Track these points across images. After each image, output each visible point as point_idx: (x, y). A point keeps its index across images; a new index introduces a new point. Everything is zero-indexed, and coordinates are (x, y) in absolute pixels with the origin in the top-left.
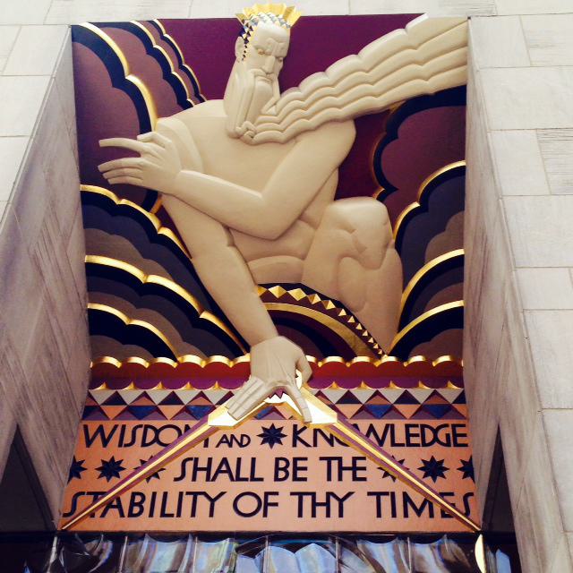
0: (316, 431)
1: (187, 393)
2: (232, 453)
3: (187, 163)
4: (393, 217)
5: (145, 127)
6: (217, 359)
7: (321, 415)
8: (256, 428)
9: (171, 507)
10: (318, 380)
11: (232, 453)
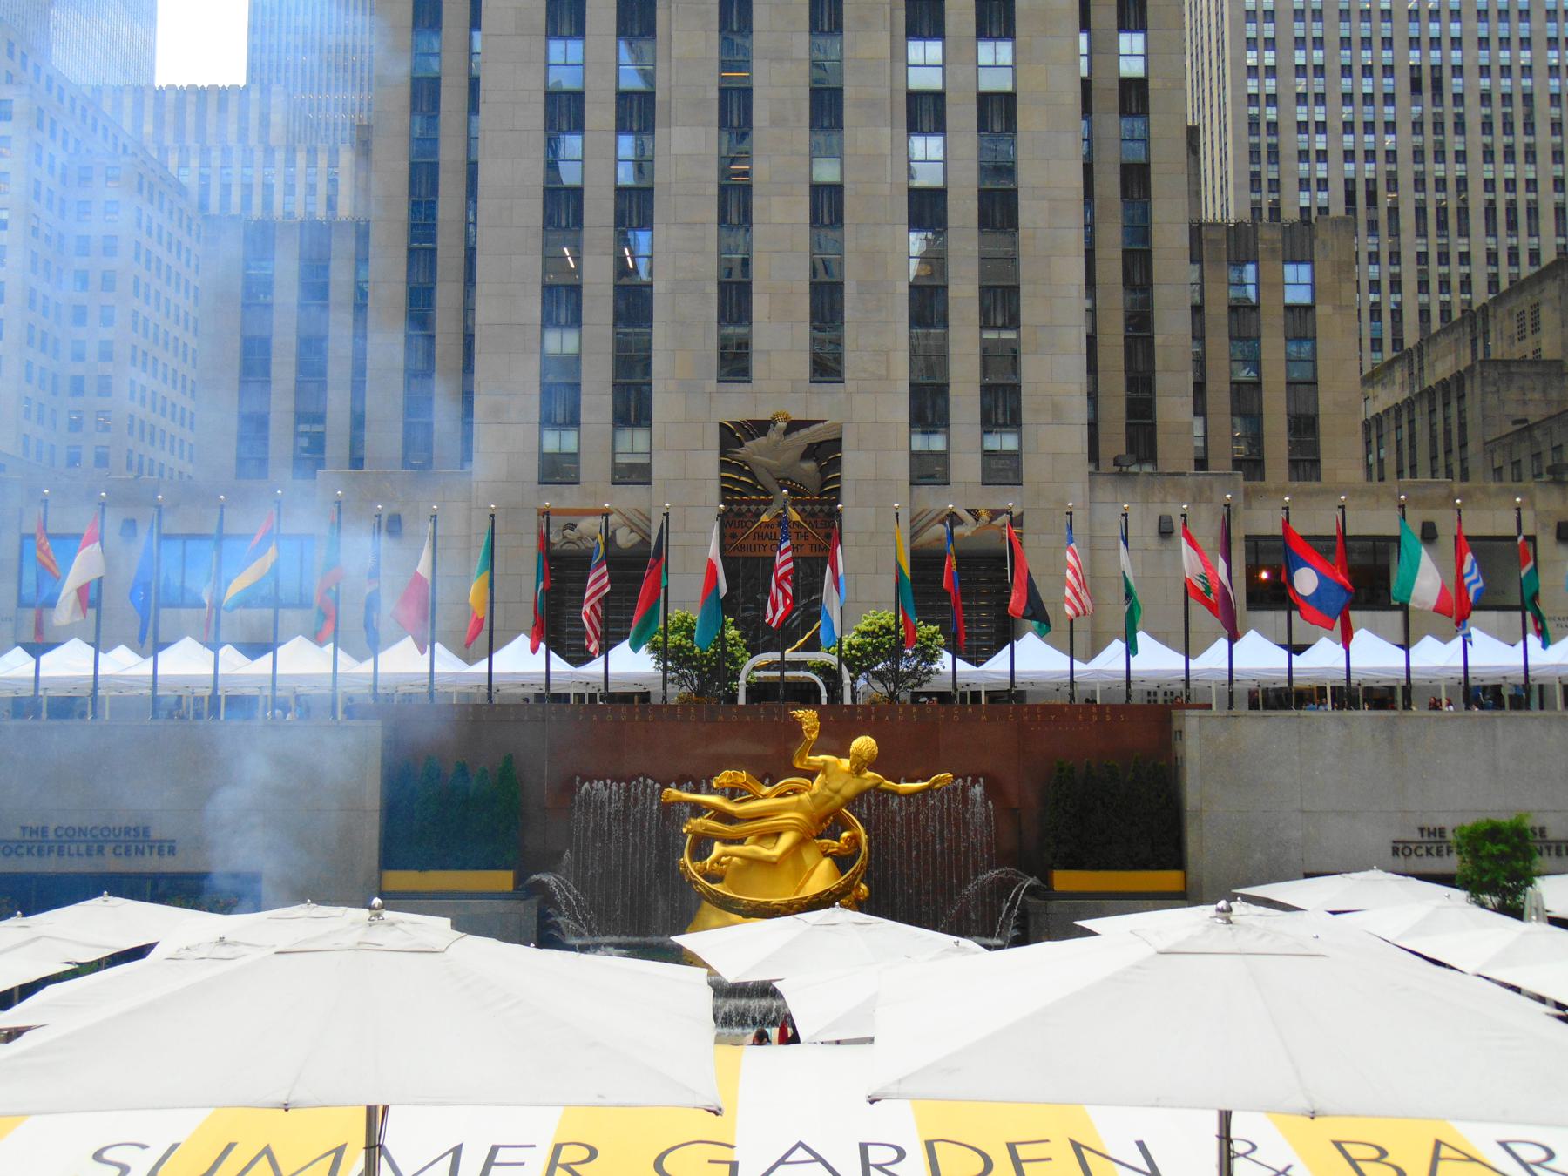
0: (794, 522)
1: (753, 508)
2: (769, 530)
3: (754, 454)
4: (818, 465)
5: (742, 445)
6: (762, 497)
7: (796, 517)
8: (775, 521)
9: (753, 549)
10: (794, 504)
11: (769, 530)
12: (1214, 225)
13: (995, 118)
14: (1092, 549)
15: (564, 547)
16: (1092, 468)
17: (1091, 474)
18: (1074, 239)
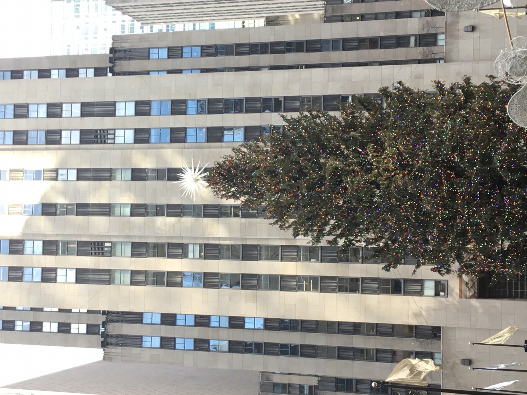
12: (326, 11)
13: (294, 105)
14: (479, 60)
15: (476, 288)
16: (442, 61)
17: (445, 62)
18: (305, 73)
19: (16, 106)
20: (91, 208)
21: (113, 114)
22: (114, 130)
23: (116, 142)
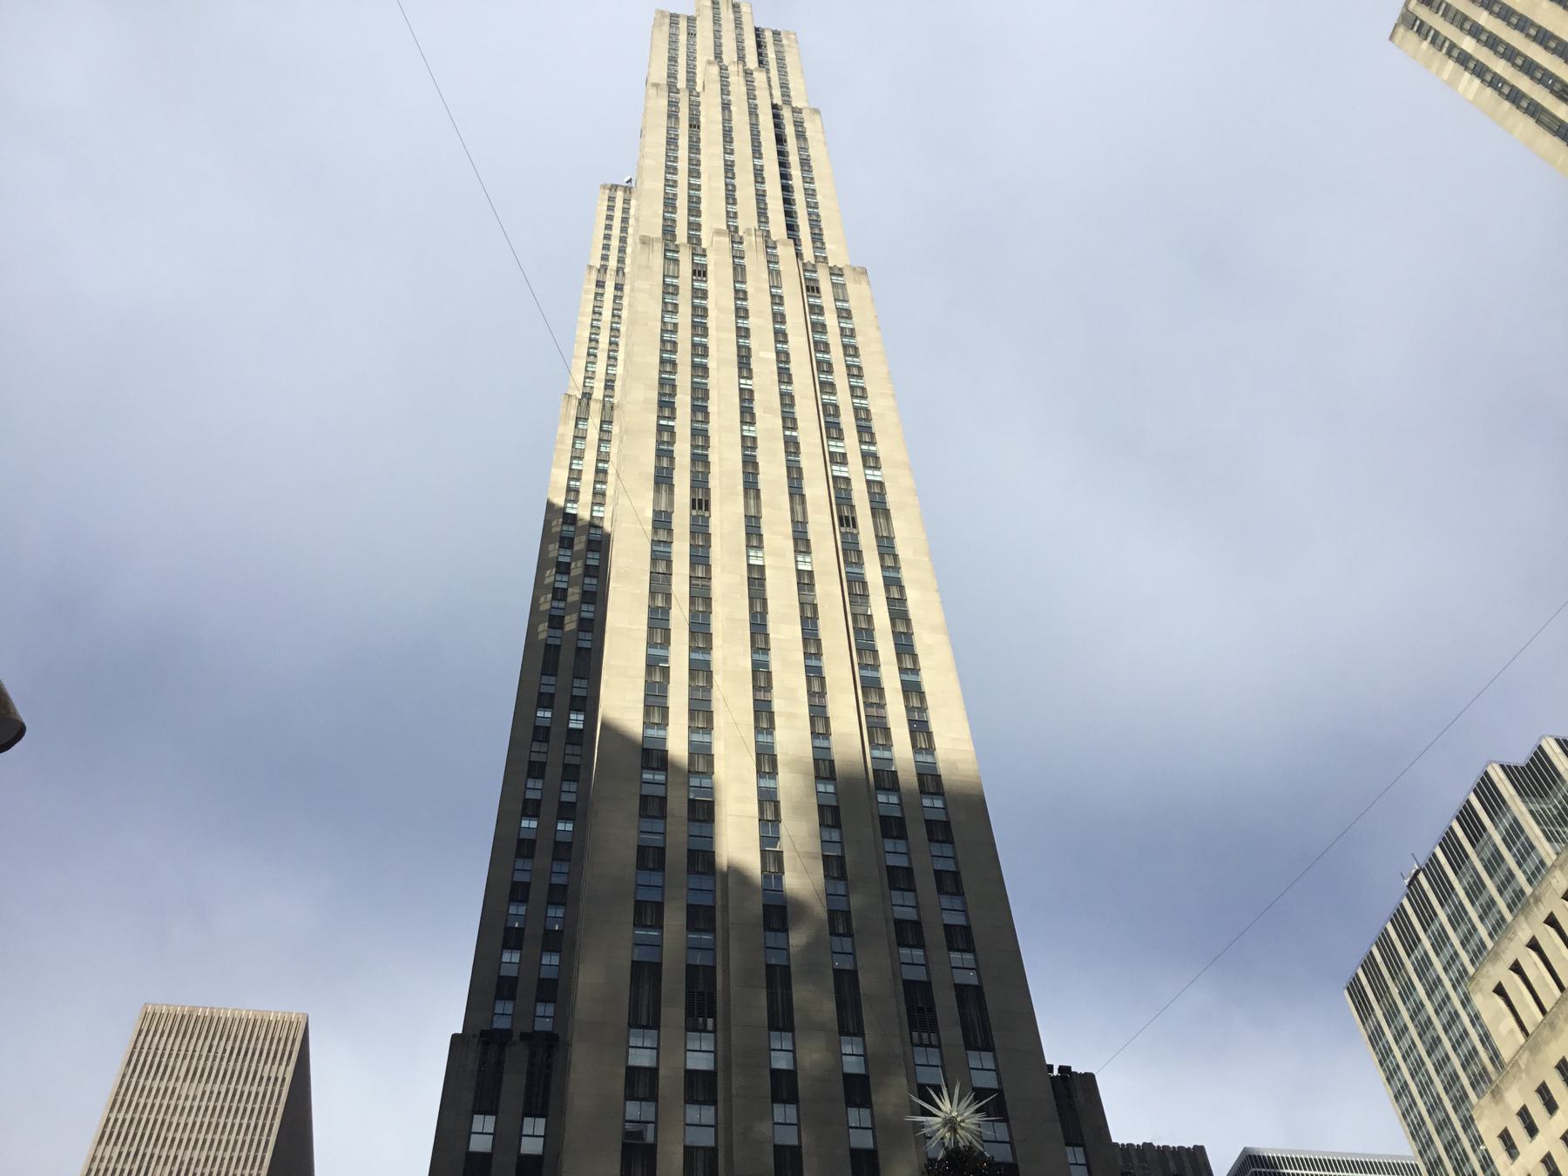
19: (956, 875)
20: (782, 993)
21: (970, 1045)
22: (939, 1046)
23: (916, 1049)
